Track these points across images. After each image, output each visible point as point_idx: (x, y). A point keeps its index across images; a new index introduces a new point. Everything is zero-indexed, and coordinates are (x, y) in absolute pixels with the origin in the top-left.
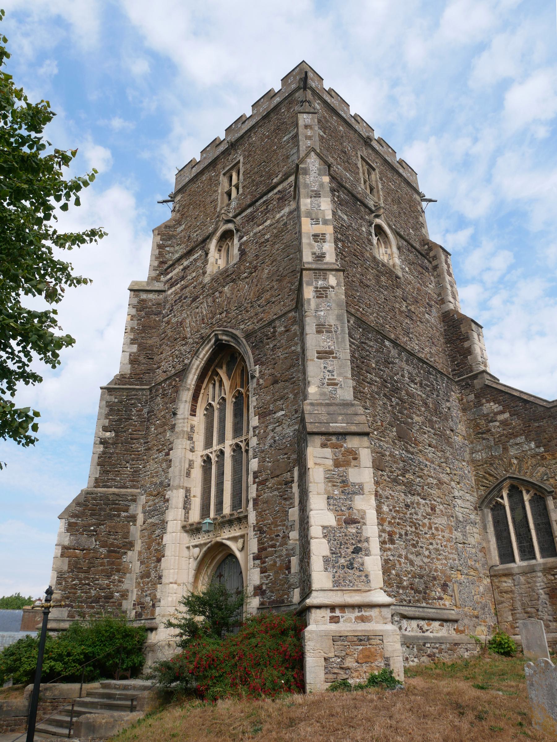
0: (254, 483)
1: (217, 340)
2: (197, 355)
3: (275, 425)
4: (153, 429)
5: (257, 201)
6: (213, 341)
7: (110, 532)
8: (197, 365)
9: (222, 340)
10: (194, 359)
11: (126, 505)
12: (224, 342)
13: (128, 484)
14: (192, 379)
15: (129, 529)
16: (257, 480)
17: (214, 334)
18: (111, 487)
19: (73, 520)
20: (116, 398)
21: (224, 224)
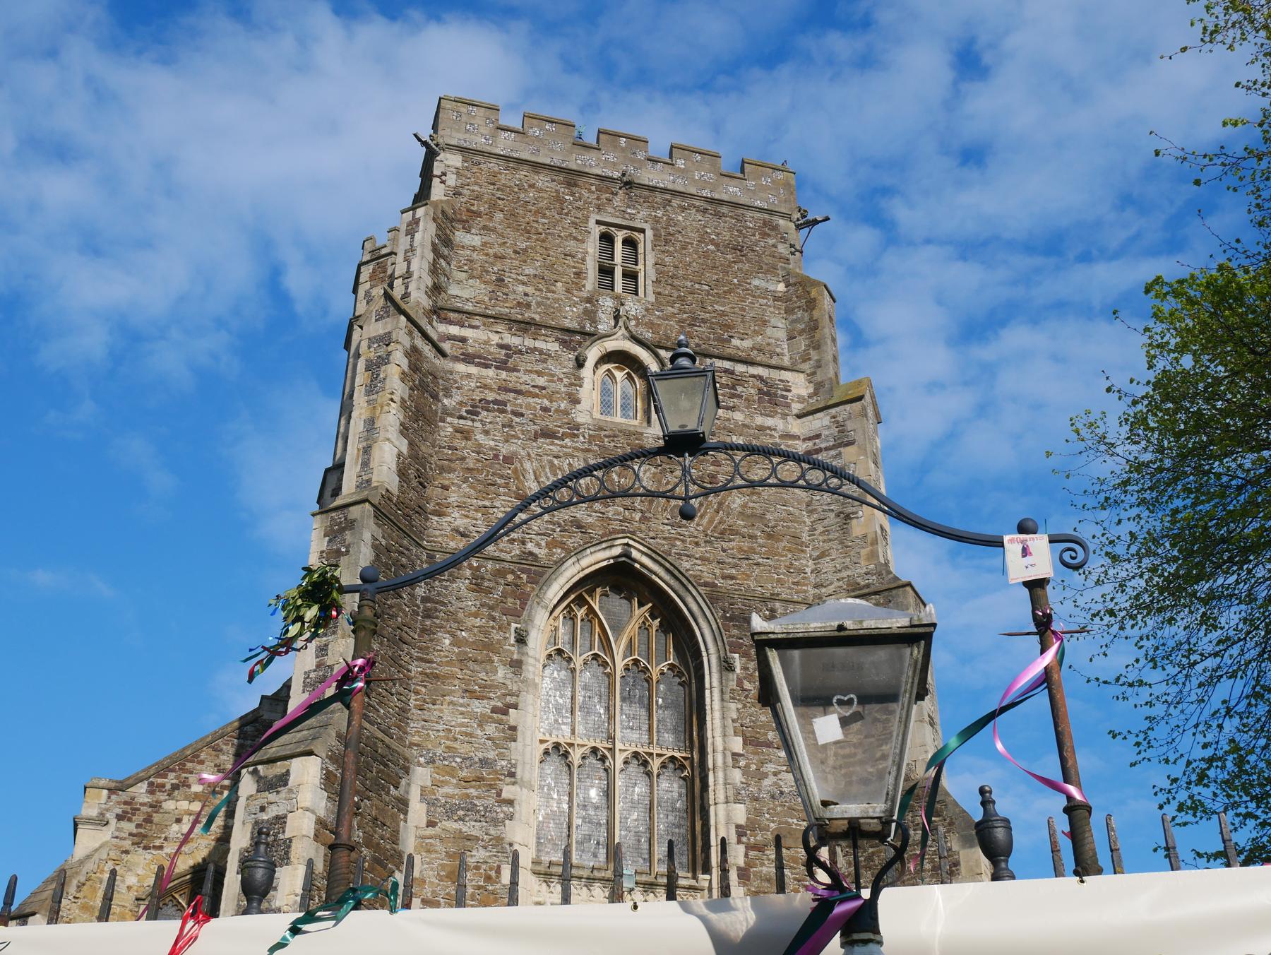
0: (739, 842)
1: (626, 554)
2: (579, 556)
3: (780, 768)
4: (447, 642)
5: (711, 356)
6: (617, 551)
7: (376, 819)
8: (572, 572)
9: (635, 561)
10: (570, 561)
11: (397, 774)
12: (637, 565)
13: (394, 730)
14: (555, 591)
15: (399, 826)
16: (744, 839)
17: (625, 541)
18: (373, 725)
19: (331, 768)
20: (383, 537)
21: (625, 338)
